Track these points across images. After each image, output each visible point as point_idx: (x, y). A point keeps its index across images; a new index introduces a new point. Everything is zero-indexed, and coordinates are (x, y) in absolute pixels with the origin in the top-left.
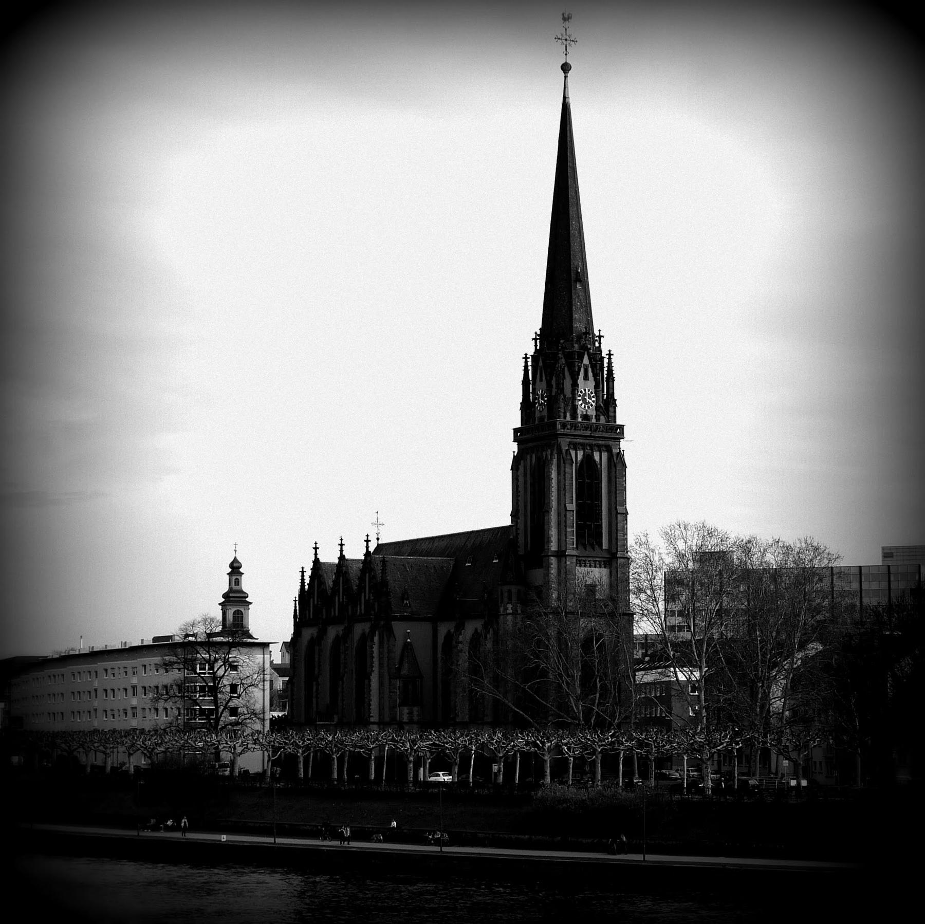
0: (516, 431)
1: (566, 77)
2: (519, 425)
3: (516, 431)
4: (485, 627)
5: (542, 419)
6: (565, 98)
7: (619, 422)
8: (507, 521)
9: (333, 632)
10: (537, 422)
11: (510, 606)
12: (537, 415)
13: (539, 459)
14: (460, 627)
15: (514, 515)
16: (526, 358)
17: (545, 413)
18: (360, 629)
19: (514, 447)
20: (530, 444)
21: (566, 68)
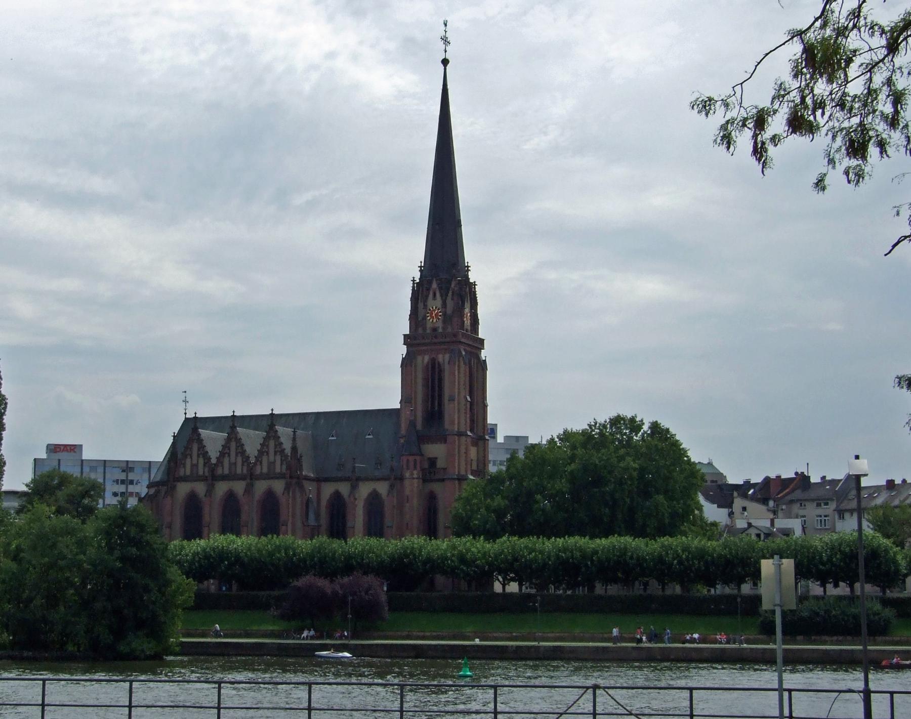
0: (405, 335)
1: (445, 69)
3: (405, 335)
4: (392, 487)
5: (435, 330)
7: (480, 336)
8: (398, 406)
9: (222, 488)
10: (428, 331)
12: (429, 325)
14: (354, 487)
15: (406, 399)
16: (414, 281)
17: (440, 325)
18: (261, 487)
19: (404, 350)
20: (425, 348)
21: (445, 62)
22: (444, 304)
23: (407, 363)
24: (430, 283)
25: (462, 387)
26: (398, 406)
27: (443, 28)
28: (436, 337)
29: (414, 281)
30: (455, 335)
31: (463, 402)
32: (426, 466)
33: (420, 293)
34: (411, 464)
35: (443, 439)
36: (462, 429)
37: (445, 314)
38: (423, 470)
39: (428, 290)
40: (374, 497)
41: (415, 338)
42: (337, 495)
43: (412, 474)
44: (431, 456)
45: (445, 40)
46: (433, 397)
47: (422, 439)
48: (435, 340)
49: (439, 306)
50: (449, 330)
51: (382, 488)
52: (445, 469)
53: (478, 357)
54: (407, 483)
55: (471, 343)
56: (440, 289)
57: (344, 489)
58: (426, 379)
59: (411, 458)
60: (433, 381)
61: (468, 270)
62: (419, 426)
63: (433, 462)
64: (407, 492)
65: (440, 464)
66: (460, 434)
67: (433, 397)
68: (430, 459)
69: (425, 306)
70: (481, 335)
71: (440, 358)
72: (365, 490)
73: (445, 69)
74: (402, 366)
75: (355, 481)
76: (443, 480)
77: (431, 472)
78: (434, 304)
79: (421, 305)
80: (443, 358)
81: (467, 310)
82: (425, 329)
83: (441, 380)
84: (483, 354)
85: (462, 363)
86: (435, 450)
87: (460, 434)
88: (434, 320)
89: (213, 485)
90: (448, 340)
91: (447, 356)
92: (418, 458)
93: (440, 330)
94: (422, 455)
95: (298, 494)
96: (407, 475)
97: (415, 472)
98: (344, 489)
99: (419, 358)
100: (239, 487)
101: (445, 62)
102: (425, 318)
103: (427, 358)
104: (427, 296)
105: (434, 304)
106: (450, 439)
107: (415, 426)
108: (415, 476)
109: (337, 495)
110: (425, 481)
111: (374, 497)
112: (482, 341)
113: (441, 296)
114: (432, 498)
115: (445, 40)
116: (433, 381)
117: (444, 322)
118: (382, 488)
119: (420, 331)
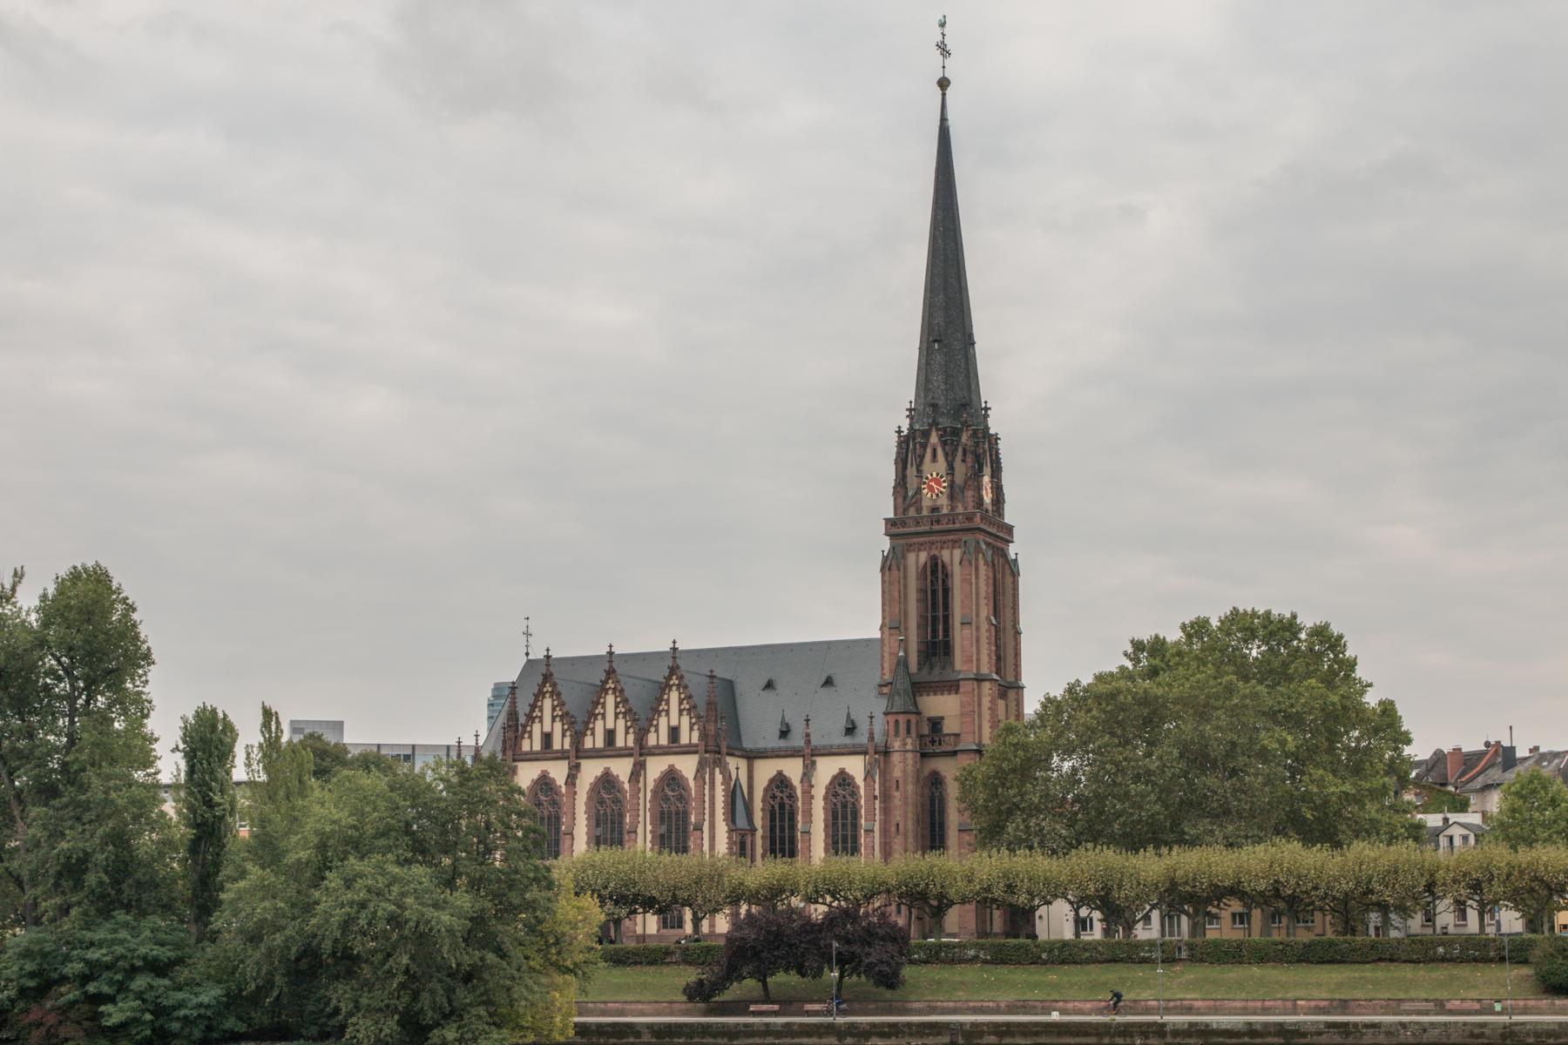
0: (887, 520)
1: (944, 95)
2: (891, 515)
3: (887, 520)
5: (935, 509)
6: (943, 119)
7: (1007, 520)
8: (878, 635)
10: (925, 513)
11: (909, 741)
13: (934, 562)
15: (893, 624)
16: (899, 432)
17: (944, 501)
18: (656, 768)
19: (886, 544)
21: (943, 84)
22: (951, 467)
23: (891, 565)
24: (926, 434)
25: (983, 602)
26: (878, 635)
27: (939, 31)
28: (938, 522)
29: (899, 432)
30: (969, 518)
31: (984, 626)
32: (926, 730)
33: (909, 450)
34: (902, 726)
35: (953, 686)
36: (985, 670)
37: (952, 485)
38: (921, 737)
39: (924, 446)
40: (842, 780)
41: (904, 524)
42: (780, 781)
43: (905, 745)
44: (933, 714)
45: (944, 50)
46: (935, 619)
47: (918, 688)
48: (936, 527)
49: (943, 471)
50: (960, 509)
51: (855, 767)
52: (957, 735)
53: (1004, 554)
54: (896, 758)
55: (994, 531)
56: (944, 444)
57: (793, 769)
58: (922, 591)
59: (902, 718)
60: (934, 592)
61: (986, 416)
62: (913, 667)
63: (936, 724)
64: (897, 773)
65: (949, 727)
66: (979, 679)
67: (935, 619)
68: (929, 719)
69: (919, 471)
70: (1007, 520)
71: (945, 555)
72: (827, 768)
73: (944, 95)
74: (882, 570)
75: (810, 754)
76: (954, 753)
77: (932, 739)
78: (935, 468)
79: (911, 471)
80: (952, 557)
81: (986, 479)
82: (919, 510)
83: (947, 591)
84: (1012, 550)
85: (981, 562)
86: (943, 705)
87: (979, 679)
88: (934, 493)
89: (578, 766)
90: (957, 526)
91: (957, 553)
92: (913, 718)
93: (945, 511)
94: (919, 713)
95: (719, 778)
96: (897, 745)
97: (909, 741)
98: (793, 769)
99: (911, 557)
100: (622, 768)
101: (943, 84)
102: (919, 491)
103: (923, 556)
104: (922, 457)
105: (935, 468)
106: (965, 686)
107: (906, 666)
108: (909, 747)
109: (780, 781)
110: (923, 755)
111: (842, 780)
112: (1010, 529)
113: (946, 455)
114: (936, 781)
115: (944, 50)
116: (934, 592)
117: (952, 497)
118: (855, 767)
119: (912, 512)
